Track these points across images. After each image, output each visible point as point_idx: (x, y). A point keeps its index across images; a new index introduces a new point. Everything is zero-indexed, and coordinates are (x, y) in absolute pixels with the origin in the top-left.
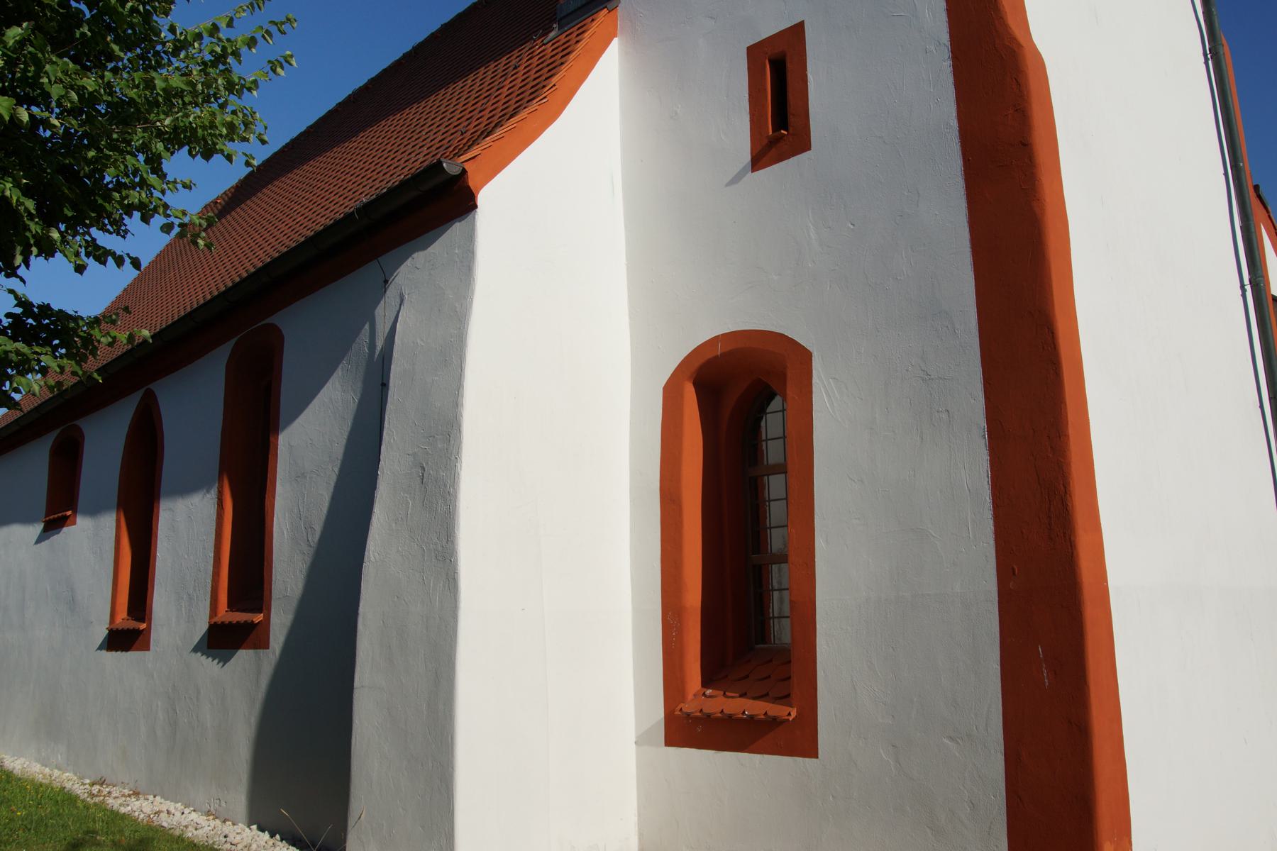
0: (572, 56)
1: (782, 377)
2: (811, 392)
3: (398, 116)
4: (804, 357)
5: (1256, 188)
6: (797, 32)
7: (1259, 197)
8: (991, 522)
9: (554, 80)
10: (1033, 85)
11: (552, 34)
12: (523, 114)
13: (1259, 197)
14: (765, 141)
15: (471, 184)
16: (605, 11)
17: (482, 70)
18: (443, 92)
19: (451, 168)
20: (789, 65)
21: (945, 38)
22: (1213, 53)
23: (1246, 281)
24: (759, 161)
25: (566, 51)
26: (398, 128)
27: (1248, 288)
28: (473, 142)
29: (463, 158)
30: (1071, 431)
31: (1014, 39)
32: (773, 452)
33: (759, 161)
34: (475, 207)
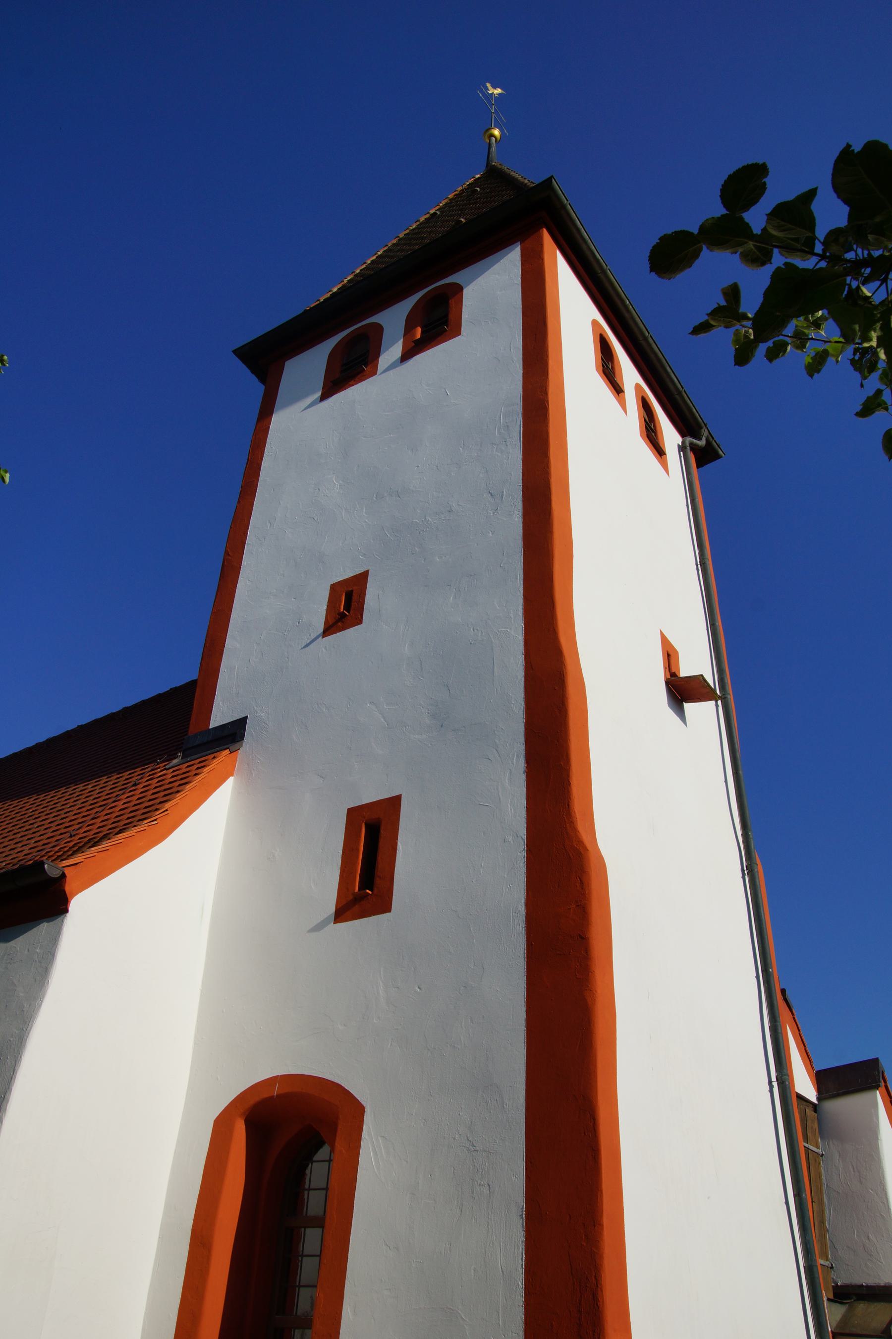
0: (188, 787)
1: (333, 1128)
2: (359, 1148)
3: (15, 803)
4: (358, 1110)
5: (783, 991)
6: (394, 803)
7: (786, 1000)
8: (522, 1310)
9: (167, 805)
10: (594, 885)
11: (175, 762)
12: (132, 832)
13: (786, 1000)
14: (351, 897)
15: (67, 889)
16: (227, 751)
17: (104, 779)
18: (63, 790)
19: (51, 869)
20: (383, 832)
21: (523, 831)
22: (750, 870)
23: (774, 1078)
24: (342, 914)
25: (184, 781)
26: (13, 815)
27: (775, 1084)
28: (79, 849)
29: (65, 863)
30: (605, 1221)
31: (581, 842)
32: (314, 1204)
33: (342, 914)
34: (67, 911)
